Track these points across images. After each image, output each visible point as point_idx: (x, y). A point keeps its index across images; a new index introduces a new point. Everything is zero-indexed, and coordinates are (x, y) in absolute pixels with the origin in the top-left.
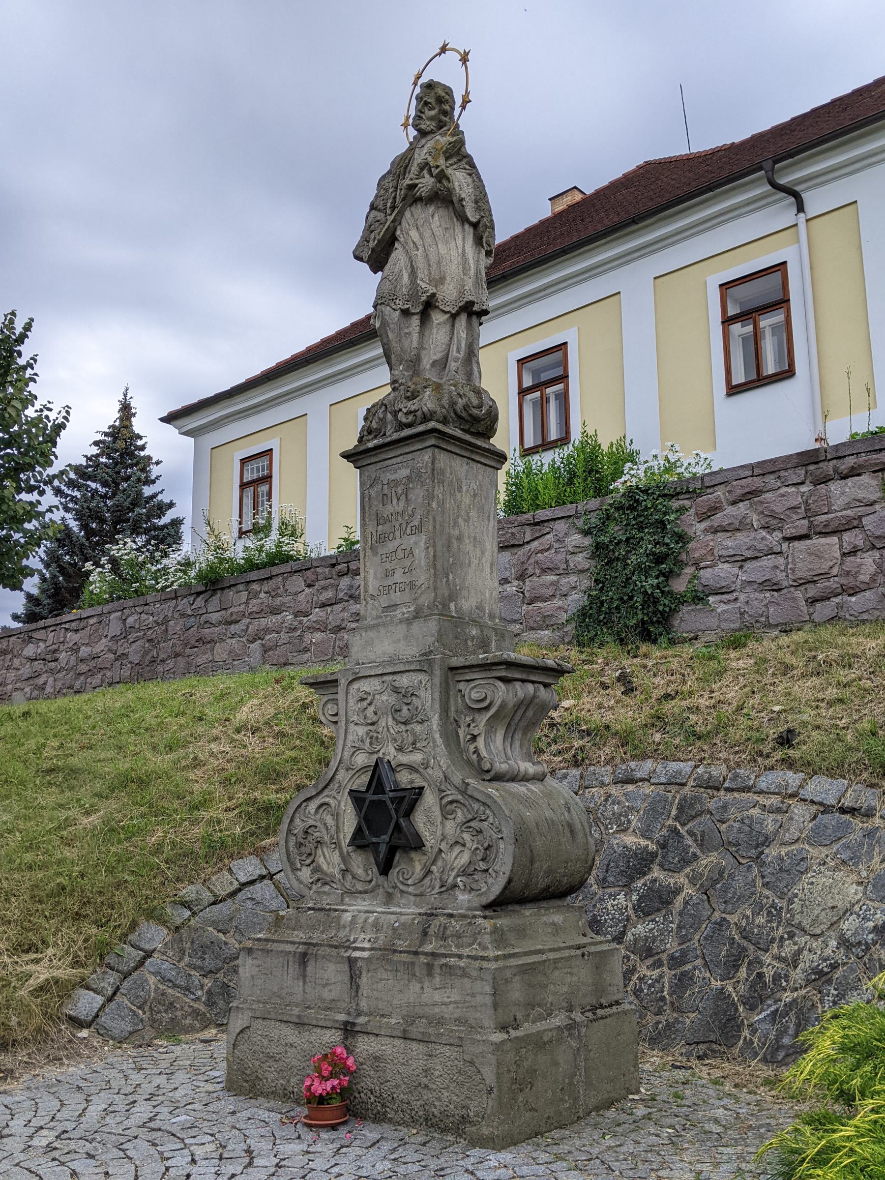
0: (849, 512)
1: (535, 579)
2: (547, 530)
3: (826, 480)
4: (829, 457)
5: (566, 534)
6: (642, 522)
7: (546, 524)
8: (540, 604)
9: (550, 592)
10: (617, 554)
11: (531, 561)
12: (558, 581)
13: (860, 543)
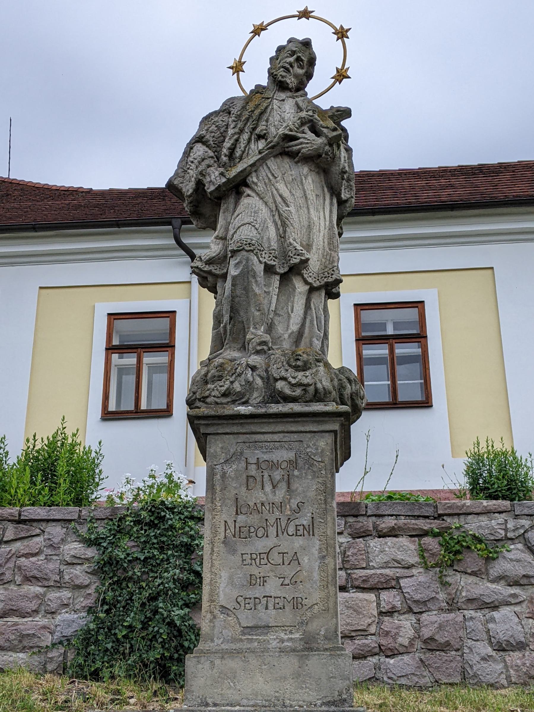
0: (387, 571)
1: (12, 587)
2: (38, 531)
3: (364, 534)
4: (370, 512)
5: (62, 539)
6: (163, 542)
7: (35, 524)
8: (16, 619)
9: (33, 605)
10: (130, 573)
11: (11, 565)
12: (44, 595)
13: (398, 604)
